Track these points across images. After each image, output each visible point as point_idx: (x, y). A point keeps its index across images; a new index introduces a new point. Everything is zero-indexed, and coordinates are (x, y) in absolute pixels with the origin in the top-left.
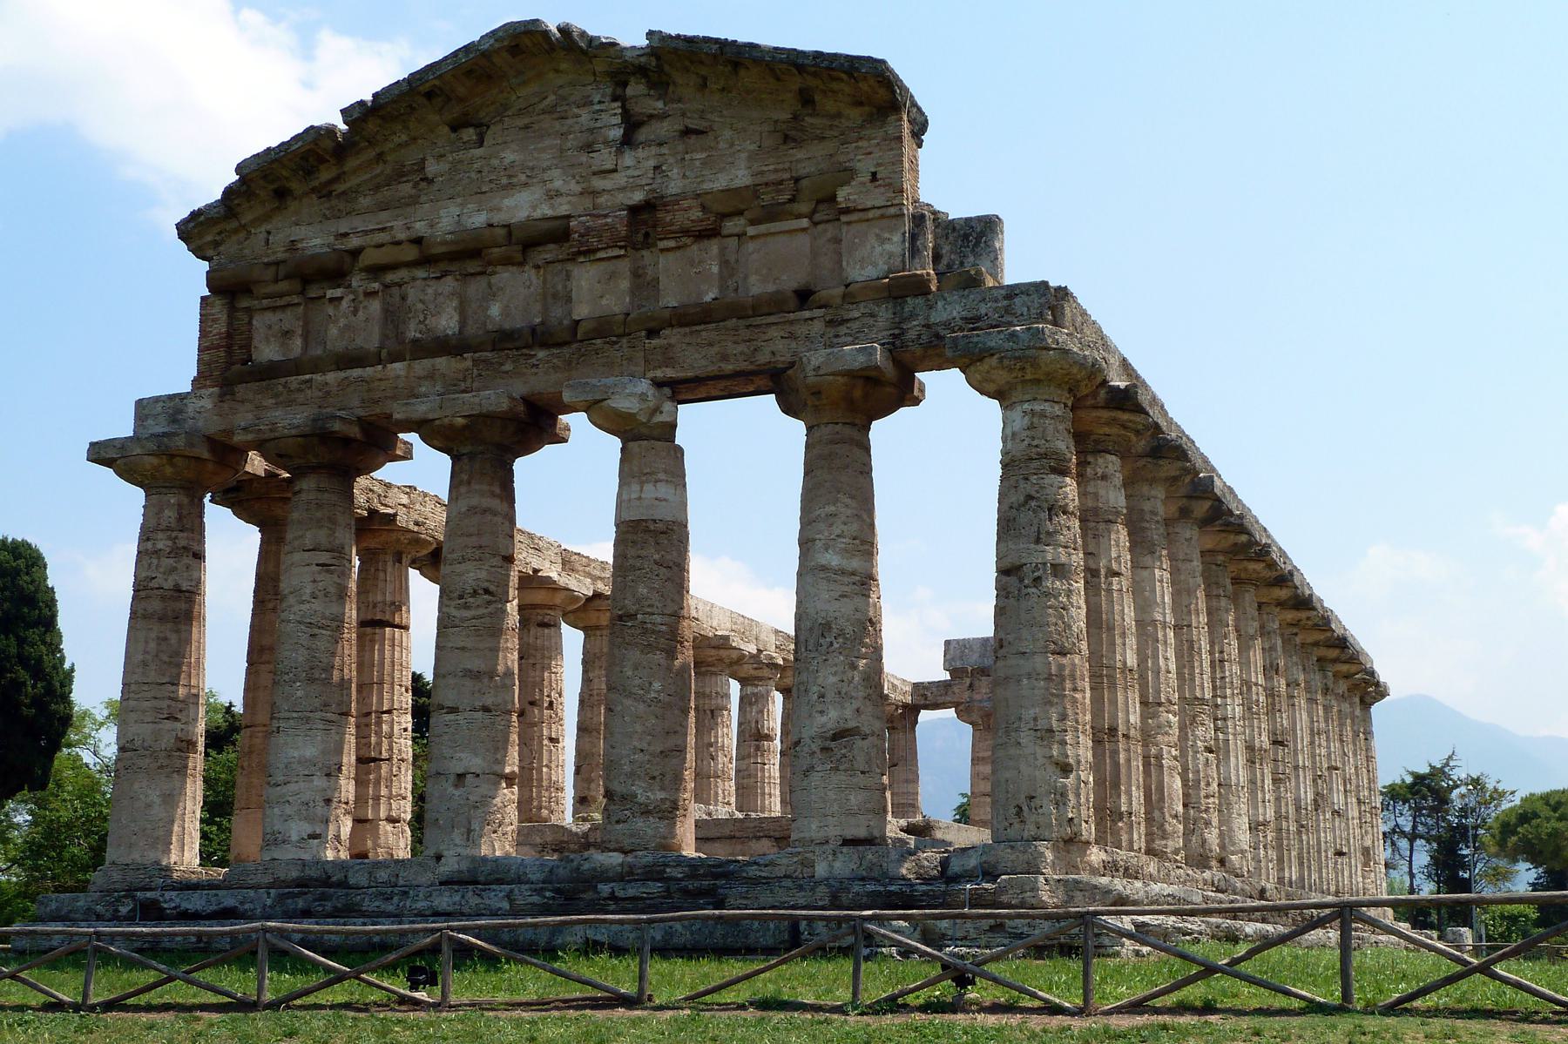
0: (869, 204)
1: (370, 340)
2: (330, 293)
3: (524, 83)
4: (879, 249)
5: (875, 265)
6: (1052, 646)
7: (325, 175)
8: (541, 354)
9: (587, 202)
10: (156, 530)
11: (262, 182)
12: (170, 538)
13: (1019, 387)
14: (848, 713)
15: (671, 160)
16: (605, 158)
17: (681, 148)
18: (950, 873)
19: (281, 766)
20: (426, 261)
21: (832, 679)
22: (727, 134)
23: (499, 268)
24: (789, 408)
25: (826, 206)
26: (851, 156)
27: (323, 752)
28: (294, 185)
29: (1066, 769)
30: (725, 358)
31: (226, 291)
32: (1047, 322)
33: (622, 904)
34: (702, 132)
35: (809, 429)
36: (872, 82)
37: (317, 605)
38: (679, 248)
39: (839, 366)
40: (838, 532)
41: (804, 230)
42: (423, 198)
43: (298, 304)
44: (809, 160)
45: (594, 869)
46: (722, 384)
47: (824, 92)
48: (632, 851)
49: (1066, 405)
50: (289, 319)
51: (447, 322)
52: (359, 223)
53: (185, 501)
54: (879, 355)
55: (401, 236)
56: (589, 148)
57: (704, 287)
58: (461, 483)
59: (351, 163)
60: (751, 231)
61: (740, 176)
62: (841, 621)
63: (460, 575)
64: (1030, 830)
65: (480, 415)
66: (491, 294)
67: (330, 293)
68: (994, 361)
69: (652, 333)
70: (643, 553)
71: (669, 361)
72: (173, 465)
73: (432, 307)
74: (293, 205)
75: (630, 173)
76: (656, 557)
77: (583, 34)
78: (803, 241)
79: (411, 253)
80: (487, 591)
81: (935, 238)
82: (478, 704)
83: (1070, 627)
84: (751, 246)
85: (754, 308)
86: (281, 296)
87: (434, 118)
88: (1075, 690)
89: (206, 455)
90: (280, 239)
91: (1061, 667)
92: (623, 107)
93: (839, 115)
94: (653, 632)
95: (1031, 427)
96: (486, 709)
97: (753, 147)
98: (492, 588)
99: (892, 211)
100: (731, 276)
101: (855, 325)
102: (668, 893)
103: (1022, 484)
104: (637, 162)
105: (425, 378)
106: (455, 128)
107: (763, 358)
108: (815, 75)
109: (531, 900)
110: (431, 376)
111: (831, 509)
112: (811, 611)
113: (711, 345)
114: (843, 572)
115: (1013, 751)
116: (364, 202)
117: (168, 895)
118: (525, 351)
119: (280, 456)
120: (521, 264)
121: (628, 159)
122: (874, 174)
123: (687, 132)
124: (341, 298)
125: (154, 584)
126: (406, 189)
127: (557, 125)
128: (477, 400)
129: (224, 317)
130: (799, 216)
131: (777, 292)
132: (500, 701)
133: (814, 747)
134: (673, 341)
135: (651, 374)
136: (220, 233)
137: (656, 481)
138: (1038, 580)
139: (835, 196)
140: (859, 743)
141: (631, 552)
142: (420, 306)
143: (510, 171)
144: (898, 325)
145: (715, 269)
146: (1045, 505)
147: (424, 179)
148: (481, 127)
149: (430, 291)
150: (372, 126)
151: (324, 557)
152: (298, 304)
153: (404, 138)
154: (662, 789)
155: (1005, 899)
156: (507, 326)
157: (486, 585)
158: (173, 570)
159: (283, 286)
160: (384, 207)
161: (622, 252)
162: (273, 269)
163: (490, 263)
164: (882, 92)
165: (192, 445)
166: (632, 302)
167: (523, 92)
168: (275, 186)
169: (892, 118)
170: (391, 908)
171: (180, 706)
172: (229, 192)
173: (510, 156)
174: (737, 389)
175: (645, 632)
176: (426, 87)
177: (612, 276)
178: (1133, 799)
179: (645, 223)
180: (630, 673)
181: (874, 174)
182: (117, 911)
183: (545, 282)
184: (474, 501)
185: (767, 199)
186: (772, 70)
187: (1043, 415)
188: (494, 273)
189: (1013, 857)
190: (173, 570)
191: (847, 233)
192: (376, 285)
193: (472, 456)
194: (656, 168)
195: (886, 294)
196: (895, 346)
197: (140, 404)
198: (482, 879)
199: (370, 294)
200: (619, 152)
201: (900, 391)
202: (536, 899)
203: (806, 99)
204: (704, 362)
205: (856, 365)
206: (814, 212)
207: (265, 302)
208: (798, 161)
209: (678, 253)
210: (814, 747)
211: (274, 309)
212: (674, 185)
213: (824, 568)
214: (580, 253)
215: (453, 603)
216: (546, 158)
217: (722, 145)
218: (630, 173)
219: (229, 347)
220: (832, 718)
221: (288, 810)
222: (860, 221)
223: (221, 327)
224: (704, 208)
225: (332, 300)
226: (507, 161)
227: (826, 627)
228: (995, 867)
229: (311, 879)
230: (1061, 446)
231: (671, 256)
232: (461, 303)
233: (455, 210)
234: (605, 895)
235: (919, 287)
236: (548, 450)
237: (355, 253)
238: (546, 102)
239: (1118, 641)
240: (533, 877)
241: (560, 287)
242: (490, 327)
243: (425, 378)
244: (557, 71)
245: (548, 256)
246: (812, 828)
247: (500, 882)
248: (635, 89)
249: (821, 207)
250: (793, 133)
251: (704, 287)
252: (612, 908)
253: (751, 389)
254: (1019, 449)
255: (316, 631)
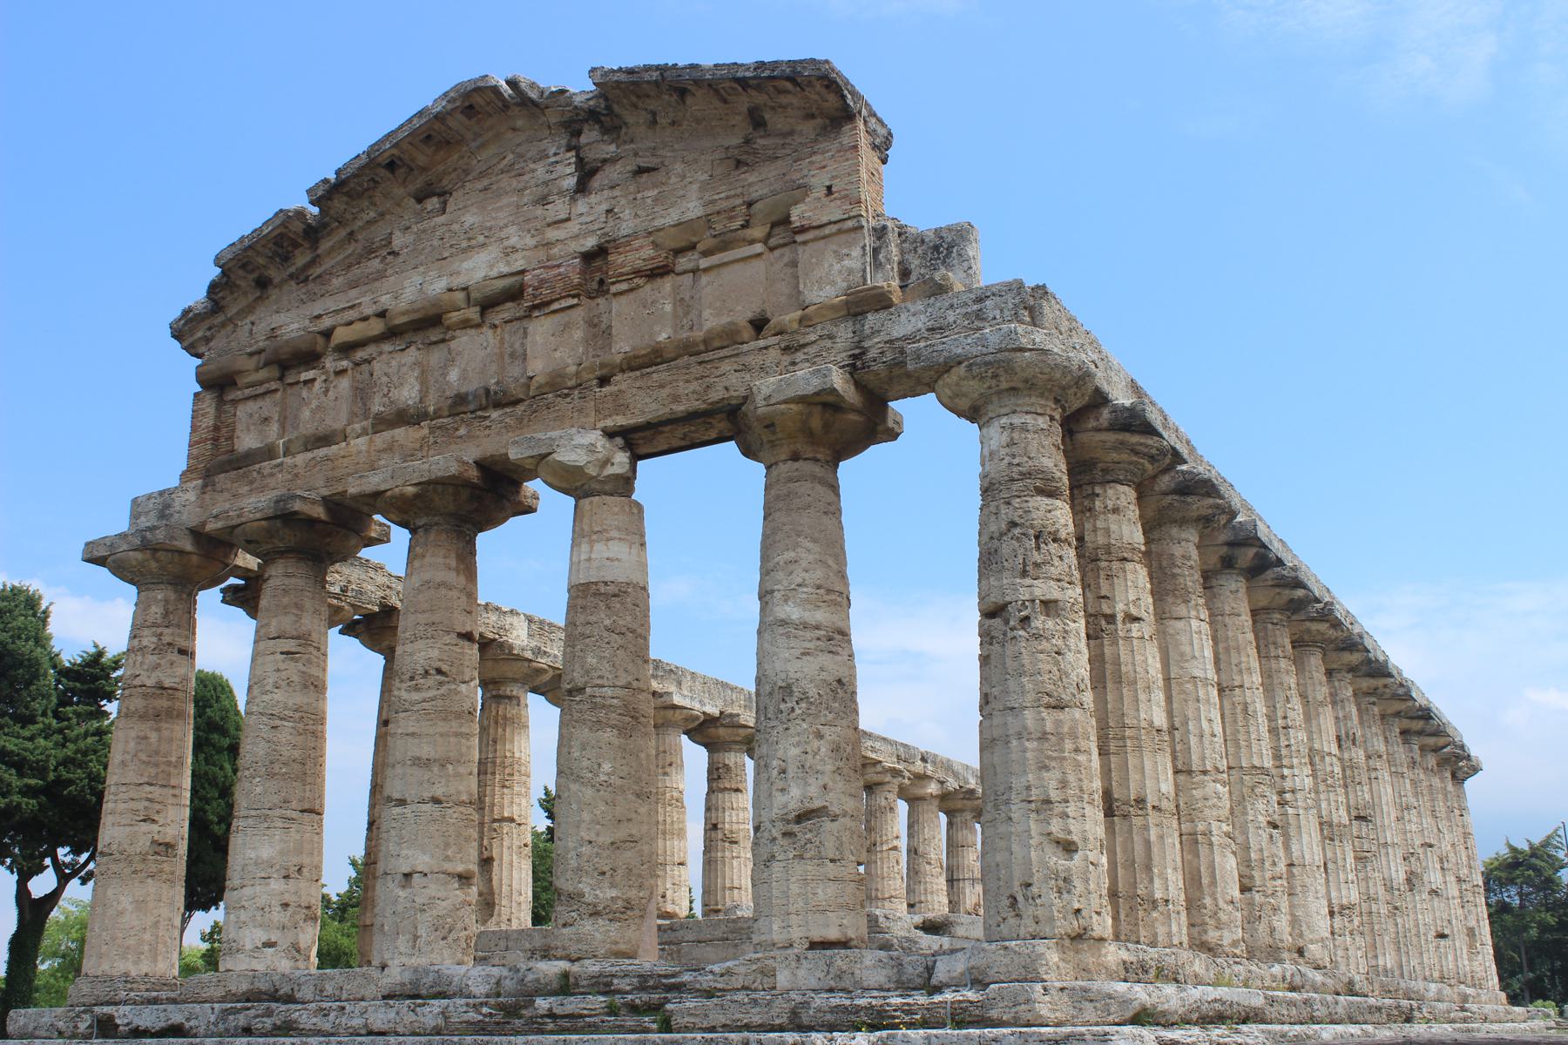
0: (825, 220)
2: (305, 376)
3: (483, 146)
4: (837, 267)
5: (833, 283)
6: (1046, 699)
7: (301, 259)
8: (495, 414)
9: (542, 254)
10: (143, 627)
11: (241, 272)
12: (155, 635)
13: (995, 399)
14: (813, 790)
15: (623, 201)
16: (559, 208)
17: (632, 189)
18: (934, 981)
19: (239, 868)
20: (392, 334)
21: (794, 751)
22: (679, 167)
23: (458, 333)
24: (748, 452)
25: (784, 230)
26: (805, 172)
27: (282, 853)
28: (274, 274)
29: (1069, 848)
30: (676, 399)
31: (217, 384)
32: (1021, 322)
33: (561, 1022)
34: (654, 169)
35: (768, 468)
36: (818, 86)
37: (279, 696)
38: (631, 290)
39: (790, 393)
40: (799, 580)
41: (759, 255)
42: (390, 271)
43: (276, 391)
44: (760, 182)
45: (538, 980)
46: (681, 431)
47: (773, 108)
48: (579, 959)
49: (1052, 419)
50: (267, 406)
51: (408, 394)
52: (331, 304)
53: (172, 596)
54: (838, 380)
55: (368, 311)
56: (543, 201)
57: (657, 328)
58: (416, 556)
59: (325, 245)
60: (704, 263)
61: (693, 208)
62: (803, 683)
63: (411, 654)
64: (1028, 926)
65: (429, 483)
66: (450, 361)
67: (305, 376)
68: (962, 369)
69: (604, 381)
70: (593, 619)
71: (621, 408)
72: (157, 561)
73: (395, 379)
74: (274, 293)
75: (583, 219)
76: (607, 622)
77: (533, 85)
78: (758, 266)
79: (377, 327)
80: (439, 671)
81: (902, 253)
82: (427, 795)
83: (1067, 675)
84: (704, 279)
85: (705, 342)
86: (261, 383)
87: (399, 191)
88: (1077, 750)
89: (189, 547)
90: (262, 329)
91: (1058, 723)
92: (577, 156)
93: (791, 133)
94: (604, 706)
95: (1011, 443)
96: (436, 801)
97: (706, 177)
98: (445, 668)
99: (850, 224)
100: (686, 314)
101: (812, 350)
102: (612, 1010)
103: (1004, 510)
104: (591, 207)
105: (384, 450)
106: (420, 200)
107: (716, 395)
108: (758, 88)
109: (466, 1017)
110: (390, 448)
111: (791, 555)
112: (770, 673)
113: (662, 386)
114: (805, 626)
115: (1002, 829)
116: (337, 282)
117: (124, 1009)
118: (479, 413)
119: (249, 542)
120: (478, 326)
121: (581, 206)
122: (829, 188)
123: (640, 171)
124: (314, 380)
125: (137, 682)
126: (375, 264)
127: (514, 183)
128: (426, 466)
129: (212, 411)
130: (752, 242)
131: (730, 323)
132: (452, 790)
133: (775, 833)
134: (623, 387)
135: (601, 424)
136: (210, 329)
137: (608, 540)
138: (1026, 619)
139: (789, 216)
140: (828, 825)
141: (581, 619)
142: (385, 379)
143: (469, 234)
144: (858, 344)
145: (668, 308)
146: (1031, 532)
147: (392, 253)
148: (444, 194)
149: (394, 363)
150: (338, 204)
151: (290, 645)
152: (276, 391)
153: (372, 214)
154: (613, 885)
155: (994, 1014)
156: (463, 390)
157: (438, 664)
158: (157, 666)
159: (263, 374)
160: (353, 285)
161: (575, 301)
162: (255, 358)
163: (448, 328)
164: (832, 98)
165: (172, 538)
166: (586, 352)
167: (483, 155)
168: (255, 275)
169: (846, 128)
170: (327, 1026)
171: (158, 807)
172: (213, 288)
173: (470, 219)
174: (699, 437)
175: (594, 706)
176: (384, 159)
177: (567, 326)
178: (1170, 883)
179: (599, 269)
180: (577, 754)
181: (829, 188)
182: (76, 1027)
183: (502, 342)
184: (427, 576)
185: (719, 227)
186: (716, 91)
187: (1024, 428)
188: (453, 338)
189: (1006, 960)
190: (157, 666)
191: (804, 254)
192: (345, 363)
193: (427, 528)
194: (609, 211)
195: (844, 312)
196: (856, 365)
197: (134, 501)
198: (424, 992)
199: (340, 373)
200: (573, 200)
201: (870, 424)
202: (473, 1016)
203: (757, 120)
204: (654, 406)
205: (810, 390)
206: (769, 236)
207: (247, 392)
208: (750, 185)
209: (631, 296)
210: (775, 833)
211: (255, 397)
212: (627, 224)
213: (783, 623)
214: (535, 307)
215: (404, 686)
216: (503, 217)
217: (673, 180)
218: (583, 219)
219: (216, 439)
220: (794, 797)
221: (243, 916)
222: (816, 239)
223: (209, 421)
224: (655, 245)
225: (306, 382)
226: (467, 225)
227: (787, 689)
228: (984, 972)
229: (260, 992)
230: (1048, 463)
231: (623, 299)
232: (423, 372)
233: (417, 279)
234: (541, 1012)
235: (881, 302)
236: (515, 523)
237: (327, 334)
238: (505, 162)
239: (1142, 697)
240: (475, 990)
241: (517, 345)
242: (448, 393)
243: (384, 450)
244: (514, 129)
245: (506, 316)
246: (775, 930)
247: (441, 995)
248: (589, 135)
249: (776, 230)
250: (744, 157)
251: (657, 328)
252: (551, 1026)
253: (714, 435)
254: (999, 469)
255: (278, 722)
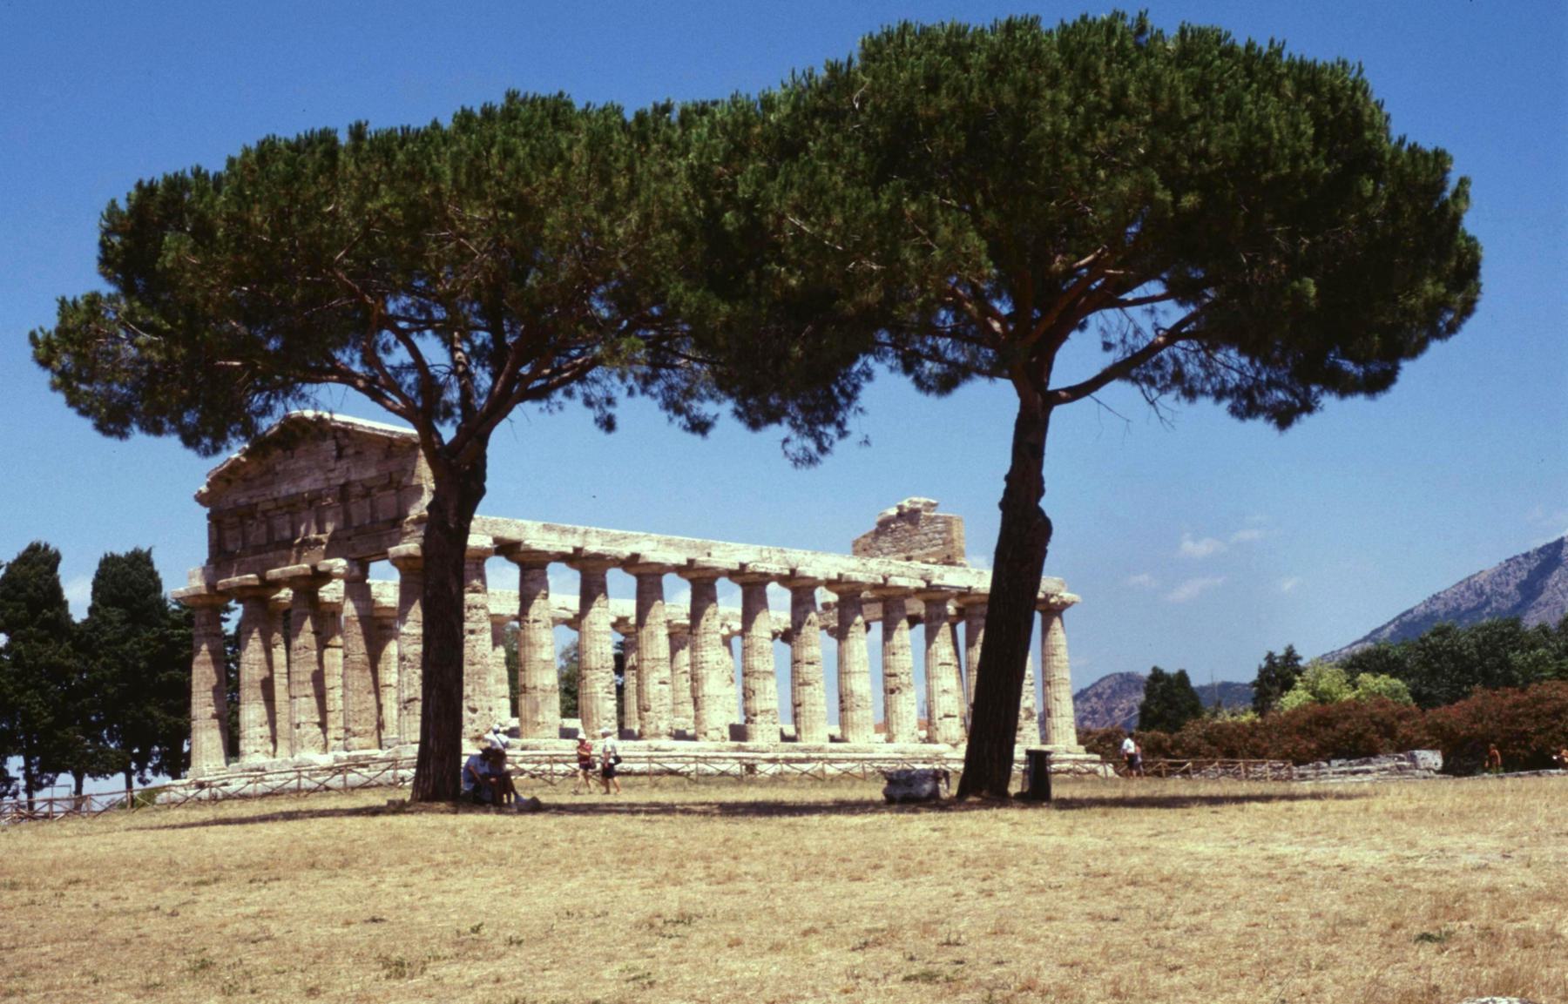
1: (263, 541)
31: (216, 521)
44: (393, 465)
61: (371, 473)
71: (354, 550)
90: (231, 499)
104: (343, 464)
116: (257, 483)
159: (235, 519)
212: (353, 477)
